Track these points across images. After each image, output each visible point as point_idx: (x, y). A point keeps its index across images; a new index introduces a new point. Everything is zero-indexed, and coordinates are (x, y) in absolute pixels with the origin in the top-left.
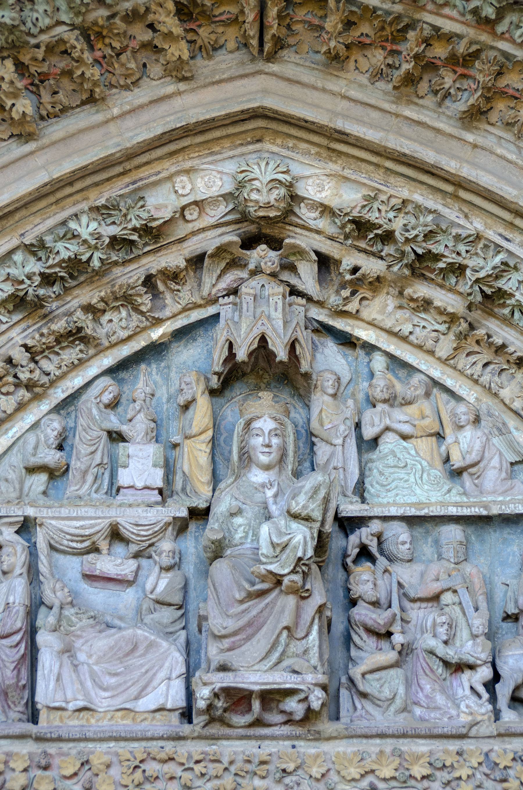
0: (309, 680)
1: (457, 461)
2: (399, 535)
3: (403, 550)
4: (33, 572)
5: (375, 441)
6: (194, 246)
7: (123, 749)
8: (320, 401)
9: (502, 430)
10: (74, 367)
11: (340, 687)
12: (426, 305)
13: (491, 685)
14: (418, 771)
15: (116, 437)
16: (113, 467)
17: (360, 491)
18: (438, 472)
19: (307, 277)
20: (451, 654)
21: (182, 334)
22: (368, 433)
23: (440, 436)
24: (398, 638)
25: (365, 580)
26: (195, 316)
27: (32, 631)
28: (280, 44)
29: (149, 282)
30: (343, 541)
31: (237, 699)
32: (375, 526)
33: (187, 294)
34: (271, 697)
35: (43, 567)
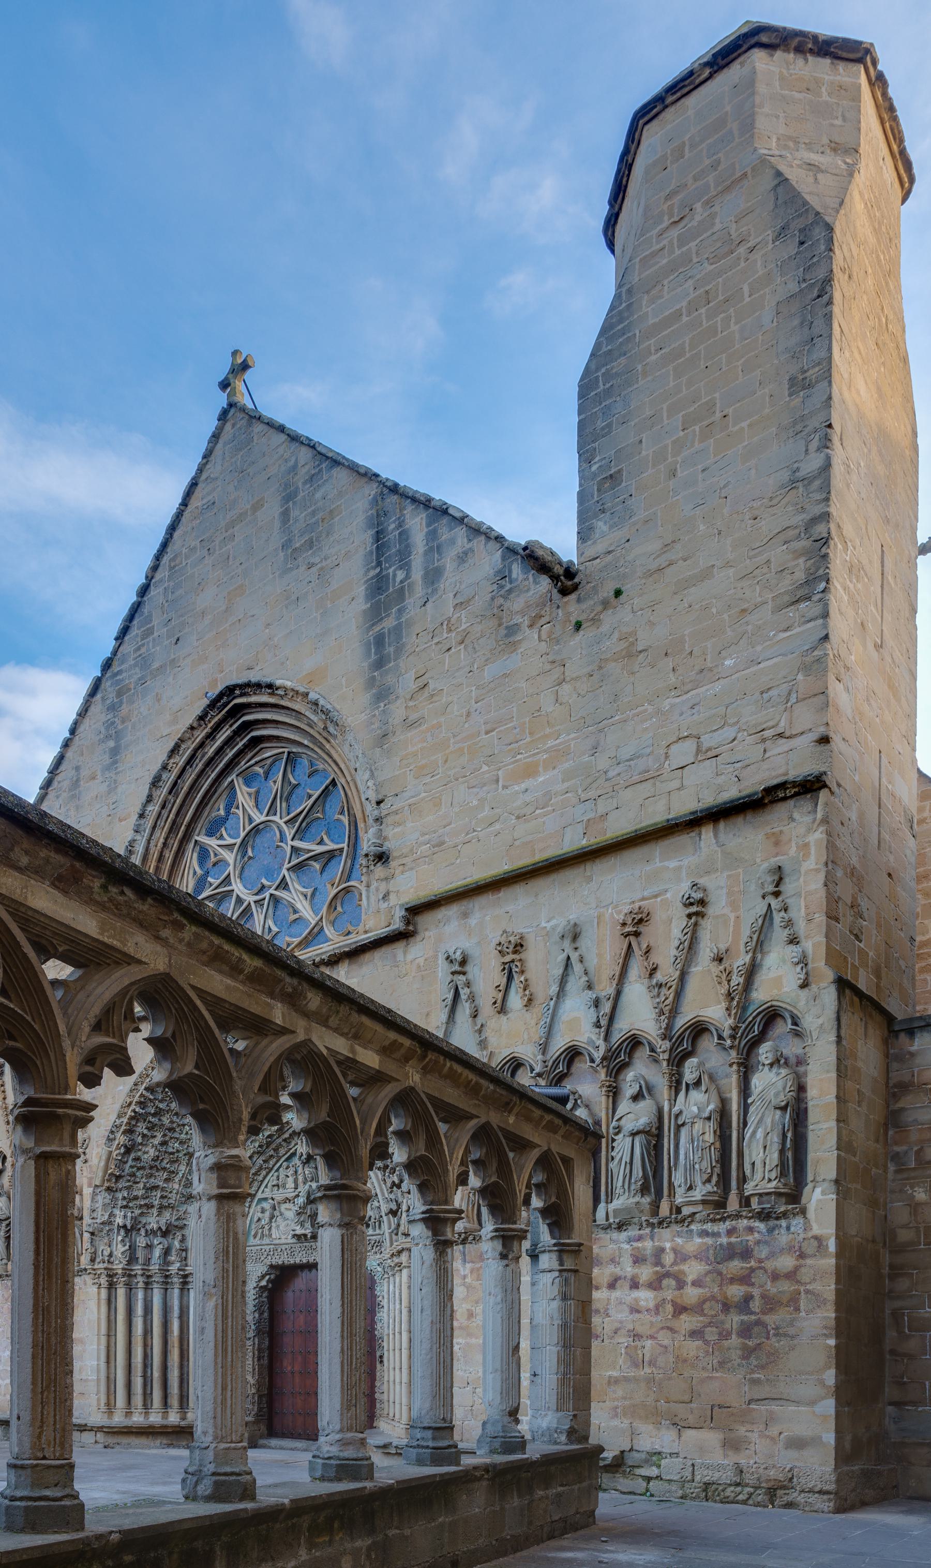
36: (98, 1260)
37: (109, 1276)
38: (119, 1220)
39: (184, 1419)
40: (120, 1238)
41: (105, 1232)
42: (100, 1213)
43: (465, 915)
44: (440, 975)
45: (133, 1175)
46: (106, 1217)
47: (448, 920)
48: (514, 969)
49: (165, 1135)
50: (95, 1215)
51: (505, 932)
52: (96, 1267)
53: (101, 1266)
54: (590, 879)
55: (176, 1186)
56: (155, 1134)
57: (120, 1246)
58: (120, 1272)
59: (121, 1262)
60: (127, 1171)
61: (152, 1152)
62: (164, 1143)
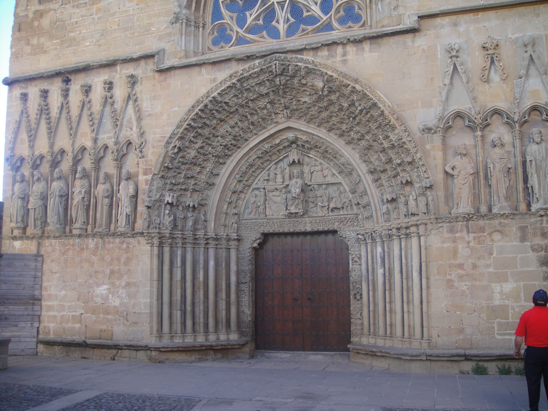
0: (301, 211)
3: (317, 189)
4: (266, 195)
5: (313, 172)
6: (284, 145)
7: (278, 220)
8: (305, 166)
9: (331, 170)
10: (269, 165)
11: (306, 212)
12: (318, 151)
13: (328, 209)
14: (318, 221)
15: (276, 174)
16: (276, 178)
18: (322, 176)
23: (322, 171)
25: (311, 194)
26: (285, 155)
29: (278, 151)
31: (292, 213)
33: (284, 152)
34: (296, 213)
36: (152, 226)
37: (160, 238)
38: (168, 199)
39: (207, 340)
40: (167, 212)
41: (156, 207)
42: (154, 194)
43: (455, 25)
44: (439, 56)
45: (178, 168)
46: (158, 196)
47: (443, 26)
48: (495, 58)
49: (203, 142)
50: (151, 194)
51: (489, 37)
52: (150, 231)
53: (154, 230)
54: (538, 16)
55: (204, 177)
56: (197, 141)
57: (167, 217)
58: (167, 235)
59: (167, 228)
60: (175, 165)
61: (193, 153)
62: (202, 148)
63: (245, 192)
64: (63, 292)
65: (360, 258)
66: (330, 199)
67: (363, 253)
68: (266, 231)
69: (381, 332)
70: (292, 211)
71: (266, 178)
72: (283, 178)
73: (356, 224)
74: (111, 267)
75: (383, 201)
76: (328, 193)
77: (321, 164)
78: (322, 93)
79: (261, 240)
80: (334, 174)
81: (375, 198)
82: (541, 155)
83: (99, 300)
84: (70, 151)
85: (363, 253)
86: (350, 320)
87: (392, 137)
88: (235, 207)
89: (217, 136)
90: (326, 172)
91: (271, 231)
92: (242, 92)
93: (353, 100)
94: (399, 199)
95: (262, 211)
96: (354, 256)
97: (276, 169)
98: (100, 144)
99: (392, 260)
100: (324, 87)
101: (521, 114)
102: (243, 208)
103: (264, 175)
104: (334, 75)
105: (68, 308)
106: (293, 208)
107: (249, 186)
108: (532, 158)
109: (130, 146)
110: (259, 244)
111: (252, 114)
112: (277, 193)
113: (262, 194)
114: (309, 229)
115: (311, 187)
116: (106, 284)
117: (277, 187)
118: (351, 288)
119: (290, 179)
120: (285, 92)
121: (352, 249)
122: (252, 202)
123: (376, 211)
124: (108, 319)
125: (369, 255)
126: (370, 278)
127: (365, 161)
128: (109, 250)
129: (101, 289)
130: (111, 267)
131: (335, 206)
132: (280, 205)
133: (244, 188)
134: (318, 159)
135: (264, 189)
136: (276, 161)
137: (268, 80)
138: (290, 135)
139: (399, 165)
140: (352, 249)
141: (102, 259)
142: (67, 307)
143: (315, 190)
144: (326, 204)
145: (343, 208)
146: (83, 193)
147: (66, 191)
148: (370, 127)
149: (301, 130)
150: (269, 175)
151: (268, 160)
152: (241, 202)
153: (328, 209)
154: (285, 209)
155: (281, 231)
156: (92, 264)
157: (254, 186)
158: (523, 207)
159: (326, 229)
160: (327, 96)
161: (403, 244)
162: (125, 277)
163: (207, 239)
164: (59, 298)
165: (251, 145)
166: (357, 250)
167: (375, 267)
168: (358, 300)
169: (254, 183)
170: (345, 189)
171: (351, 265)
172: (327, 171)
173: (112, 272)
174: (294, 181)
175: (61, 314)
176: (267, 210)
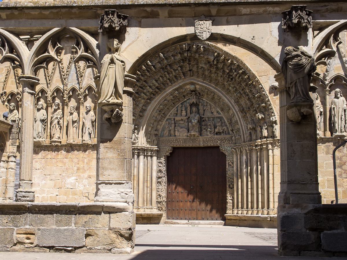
1: (212, 112)
2: (207, 119)
4: (175, 123)
5: (205, 110)
16: (182, 112)
17: (204, 115)
19: (198, 95)
20: (210, 130)
21: (188, 100)
22: (204, 109)
23: (211, 109)
24: (206, 129)
25: (203, 123)
26: (187, 98)
27: (175, 129)
28: (193, 75)
30: (201, 121)
32: (205, 118)
34: (194, 135)
35: (176, 122)
63: (162, 120)
64: (44, 182)
65: (233, 163)
66: (215, 127)
67: (235, 160)
68: (175, 146)
69: (245, 207)
70: (192, 133)
71: (176, 112)
72: (186, 112)
73: (230, 142)
74: (78, 166)
75: (247, 129)
76: (214, 122)
77: (210, 104)
78: (213, 63)
79: (172, 151)
80: (218, 112)
81: (243, 127)
82: (340, 104)
83: (70, 186)
84: (49, 91)
85: (235, 160)
86: (226, 200)
87: (254, 91)
88: (156, 130)
89: (147, 86)
90: (213, 110)
91: (178, 146)
92: (163, 60)
93: (231, 68)
94: (257, 128)
95: (173, 133)
96: (229, 161)
97: (182, 107)
98: (69, 87)
99: (252, 164)
100: (214, 60)
101: (329, 80)
102: (160, 130)
103: (173, 111)
104: (221, 53)
105: (47, 192)
106: (192, 132)
107: (165, 118)
108: (335, 106)
109: (90, 90)
110: (170, 153)
111: (168, 74)
112: (183, 122)
113: (173, 122)
114: (202, 145)
115: (203, 119)
116: (74, 176)
117: (182, 118)
118: (227, 180)
119: (191, 113)
120: (189, 61)
121: (228, 158)
122: (167, 127)
123: (243, 134)
124: (75, 198)
125: (239, 161)
126: (239, 174)
127: (237, 105)
128: (76, 155)
129: (71, 179)
130: (78, 166)
131: (218, 131)
132: (184, 129)
133: (162, 119)
134: (208, 101)
135: (174, 119)
136: (182, 102)
137: (180, 53)
138: (192, 87)
139: (258, 108)
140: (228, 158)
141: (72, 161)
142: (46, 191)
143: (206, 121)
144: (213, 129)
145: (223, 132)
146: (59, 118)
147: (46, 117)
148: (241, 84)
149: (198, 84)
150: (177, 111)
151: (177, 101)
152: (159, 127)
153: (214, 132)
154: (187, 132)
155: (184, 146)
156: (65, 164)
157: (168, 117)
158: (328, 134)
159: (212, 145)
160: (216, 65)
161: (258, 153)
162: (88, 172)
163: (139, 150)
164: (40, 185)
165: (167, 92)
166: (231, 158)
167: (242, 167)
168: (231, 188)
169: (168, 116)
170: (224, 121)
171: (227, 167)
172: (214, 109)
173: (78, 169)
174: (193, 115)
175: (42, 195)
176: (176, 132)
